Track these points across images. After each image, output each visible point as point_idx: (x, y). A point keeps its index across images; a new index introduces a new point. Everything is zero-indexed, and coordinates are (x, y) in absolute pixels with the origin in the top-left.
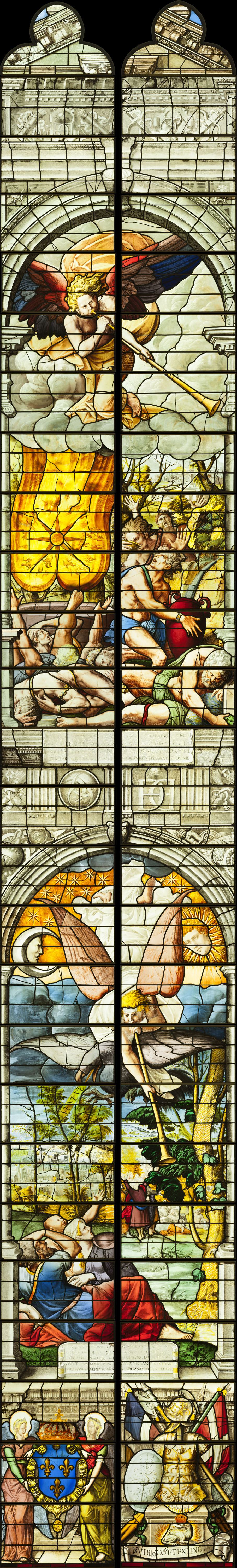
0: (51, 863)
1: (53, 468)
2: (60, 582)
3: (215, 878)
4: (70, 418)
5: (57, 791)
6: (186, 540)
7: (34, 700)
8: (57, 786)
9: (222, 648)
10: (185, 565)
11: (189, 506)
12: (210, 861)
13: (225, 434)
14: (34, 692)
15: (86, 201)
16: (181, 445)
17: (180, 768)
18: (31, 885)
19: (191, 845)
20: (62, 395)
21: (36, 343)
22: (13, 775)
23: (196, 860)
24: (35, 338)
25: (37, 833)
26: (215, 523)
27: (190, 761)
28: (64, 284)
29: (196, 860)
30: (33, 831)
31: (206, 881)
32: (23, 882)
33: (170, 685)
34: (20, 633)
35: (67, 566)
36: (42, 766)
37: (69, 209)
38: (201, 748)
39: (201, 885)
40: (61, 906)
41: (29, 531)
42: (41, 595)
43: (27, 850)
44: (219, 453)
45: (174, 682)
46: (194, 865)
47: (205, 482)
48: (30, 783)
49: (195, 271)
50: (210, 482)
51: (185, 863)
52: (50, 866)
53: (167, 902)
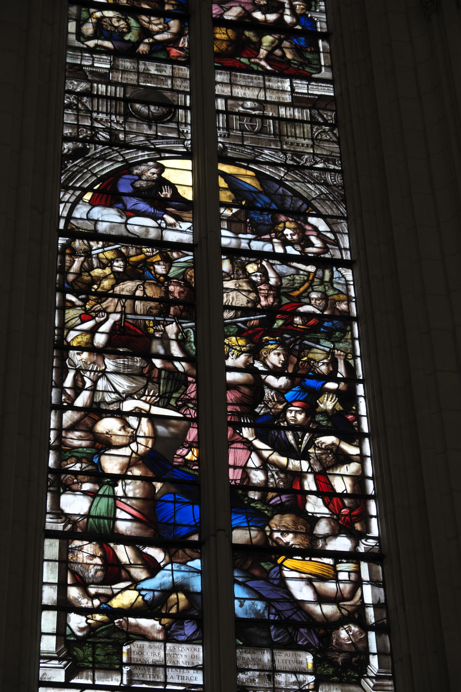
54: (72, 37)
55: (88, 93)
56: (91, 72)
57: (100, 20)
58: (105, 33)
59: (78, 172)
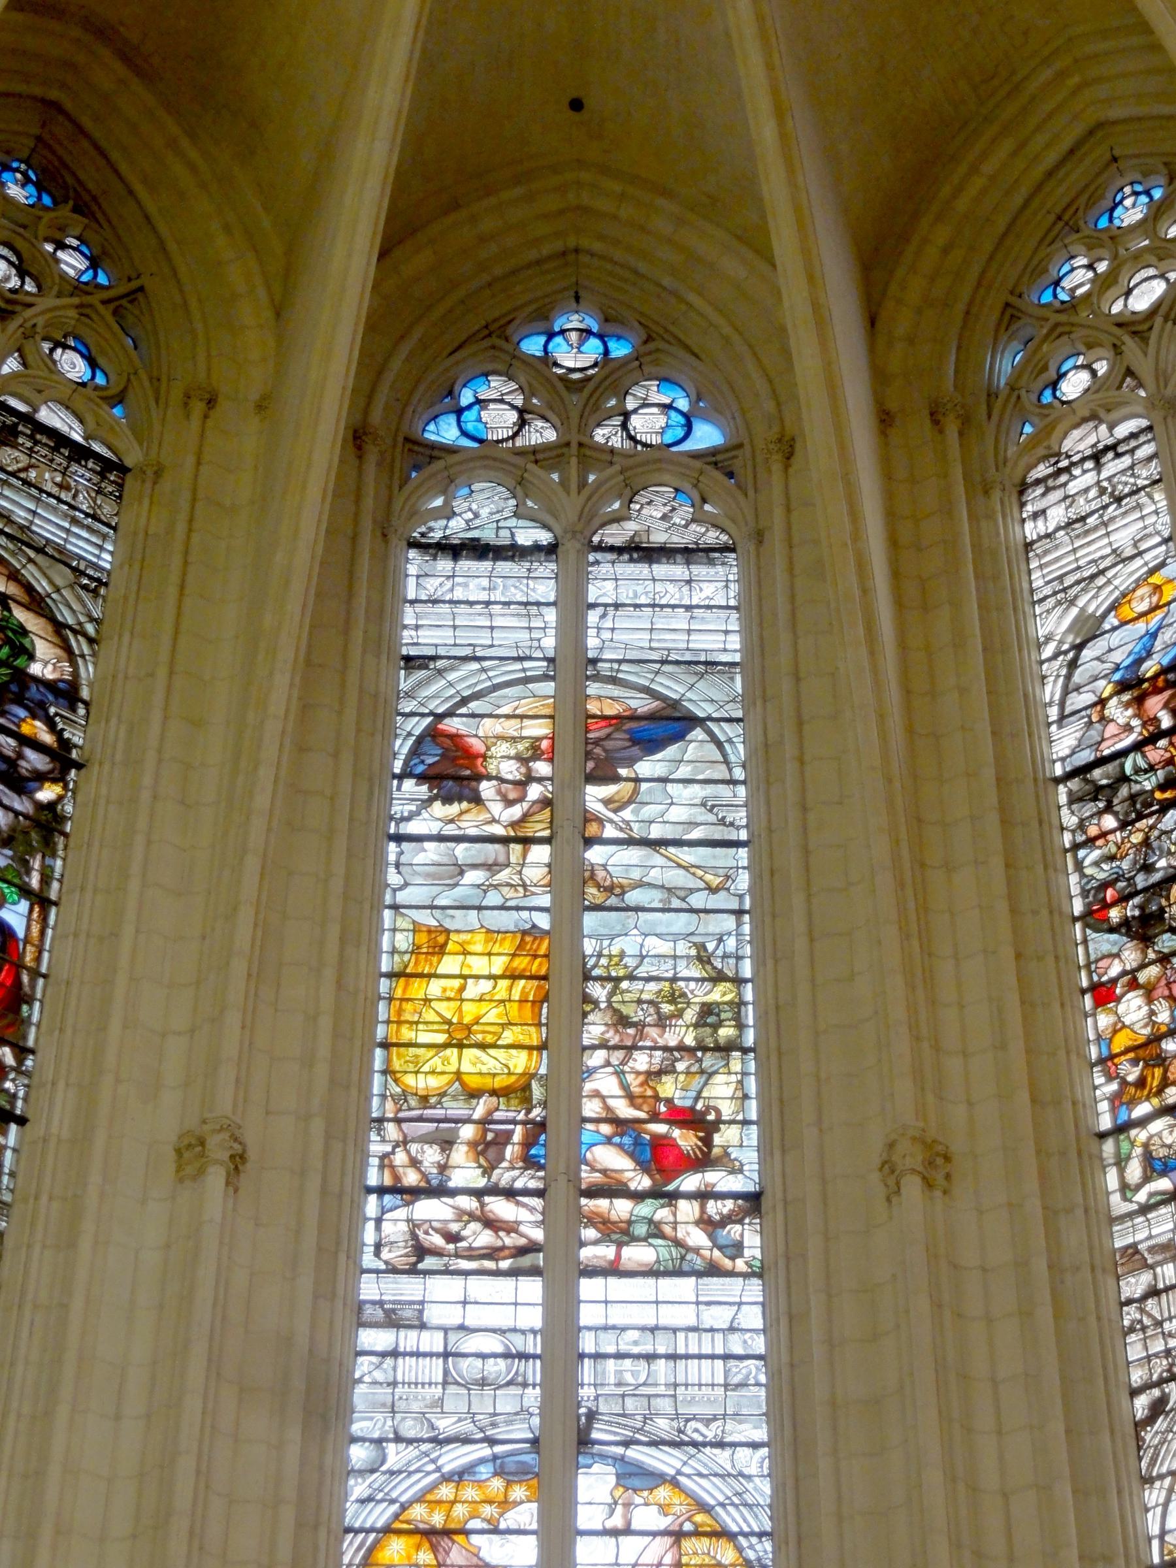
0: (431, 1467)
1: (458, 948)
2: (463, 1084)
3: (737, 1494)
4: (485, 892)
5: (445, 1362)
6: (683, 1033)
7: (414, 1236)
8: (446, 1355)
9: (741, 1171)
10: (681, 1066)
11: (683, 995)
12: (728, 1467)
13: (739, 913)
14: (414, 1225)
15: (517, 666)
16: (669, 924)
17: (675, 1331)
18: (393, 1501)
19: (694, 1444)
20: (475, 866)
21: (438, 809)
22: (371, 1338)
23: (705, 1465)
24: (437, 805)
25: (409, 1423)
26: (723, 1016)
27: (692, 1321)
28: (482, 749)
29: (705, 1465)
30: (404, 1419)
31: (721, 1498)
32: (380, 1496)
33: (657, 1217)
34: (397, 1145)
35: (474, 1064)
36: (423, 1326)
37: (491, 674)
38: (708, 1304)
39: (712, 1502)
40: (447, 1533)
41: (417, 1023)
42: (433, 1100)
43: (391, 1448)
44: (730, 934)
45: (663, 1214)
46: (700, 1475)
47: (708, 967)
48: (402, 1349)
49: (688, 737)
50: (715, 968)
51: (686, 1470)
52: (428, 1473)
53: (654, 1528)
54: (1116, 1198)
55: (1154, 1292)
56: (1151, 1250)
57: (1146, 1146)
58: (1158, 1165)
59: (1162, 1443)
